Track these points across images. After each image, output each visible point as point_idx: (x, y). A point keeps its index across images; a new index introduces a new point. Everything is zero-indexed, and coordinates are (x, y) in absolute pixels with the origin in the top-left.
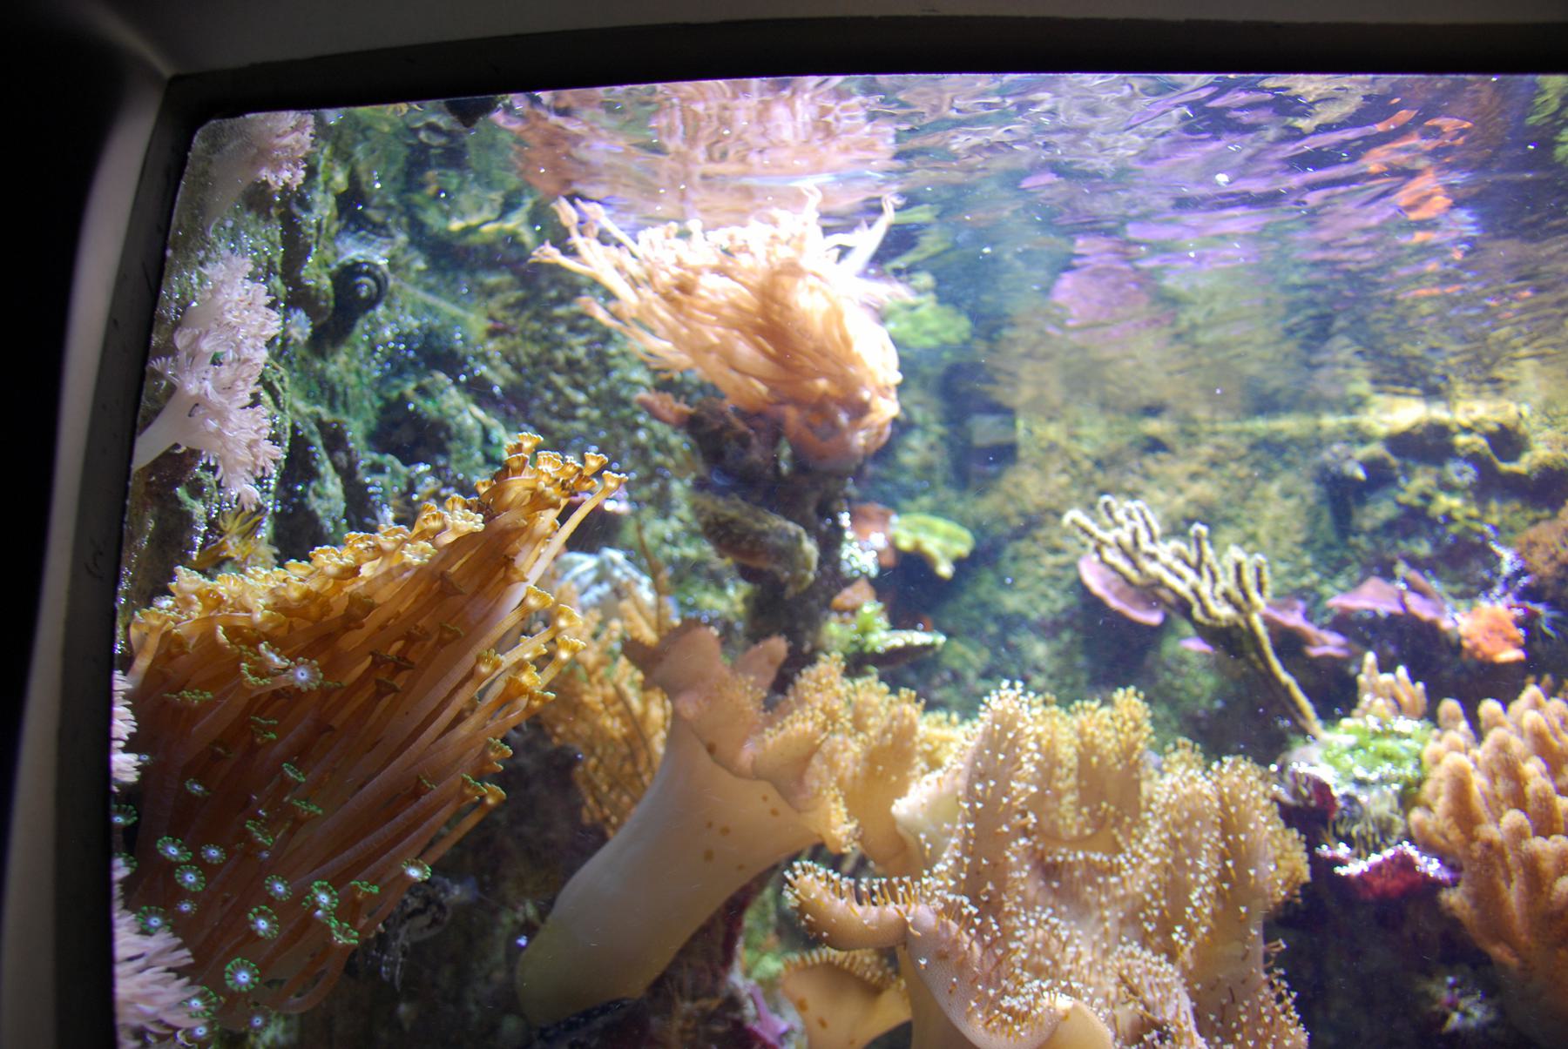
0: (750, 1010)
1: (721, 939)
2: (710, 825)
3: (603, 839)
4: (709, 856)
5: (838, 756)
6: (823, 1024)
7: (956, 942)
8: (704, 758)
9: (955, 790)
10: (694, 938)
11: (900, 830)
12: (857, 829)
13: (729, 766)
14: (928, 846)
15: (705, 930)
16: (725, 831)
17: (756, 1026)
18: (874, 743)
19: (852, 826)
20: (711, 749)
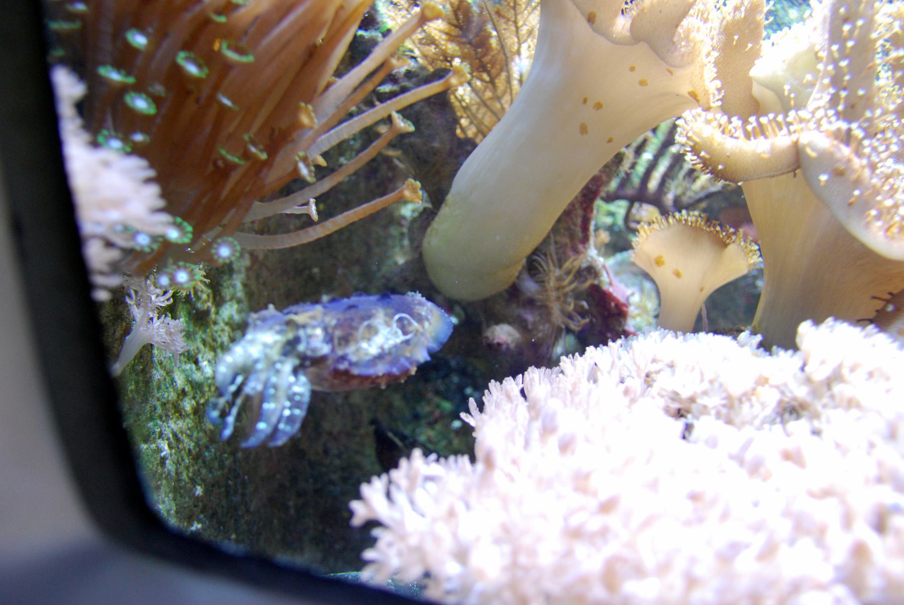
0: (605, 278)
1: (579, 221)
2: (585, 101)
3: (474, 146)
4: (584, 129)
5: (692, 35)
6: (678, 274)
7: (849, 161)
8: (581, 26)
9: (811, 49)
10: (559, 220)
11: (756, 90)
12: (719, 90)
13: (606, 34)
14: (792, 95)
15: (567, 213)
16: (598, 106)
17: (611, 290)
18: (729, 18)
19: (718, 84)
20: (591, 19)
